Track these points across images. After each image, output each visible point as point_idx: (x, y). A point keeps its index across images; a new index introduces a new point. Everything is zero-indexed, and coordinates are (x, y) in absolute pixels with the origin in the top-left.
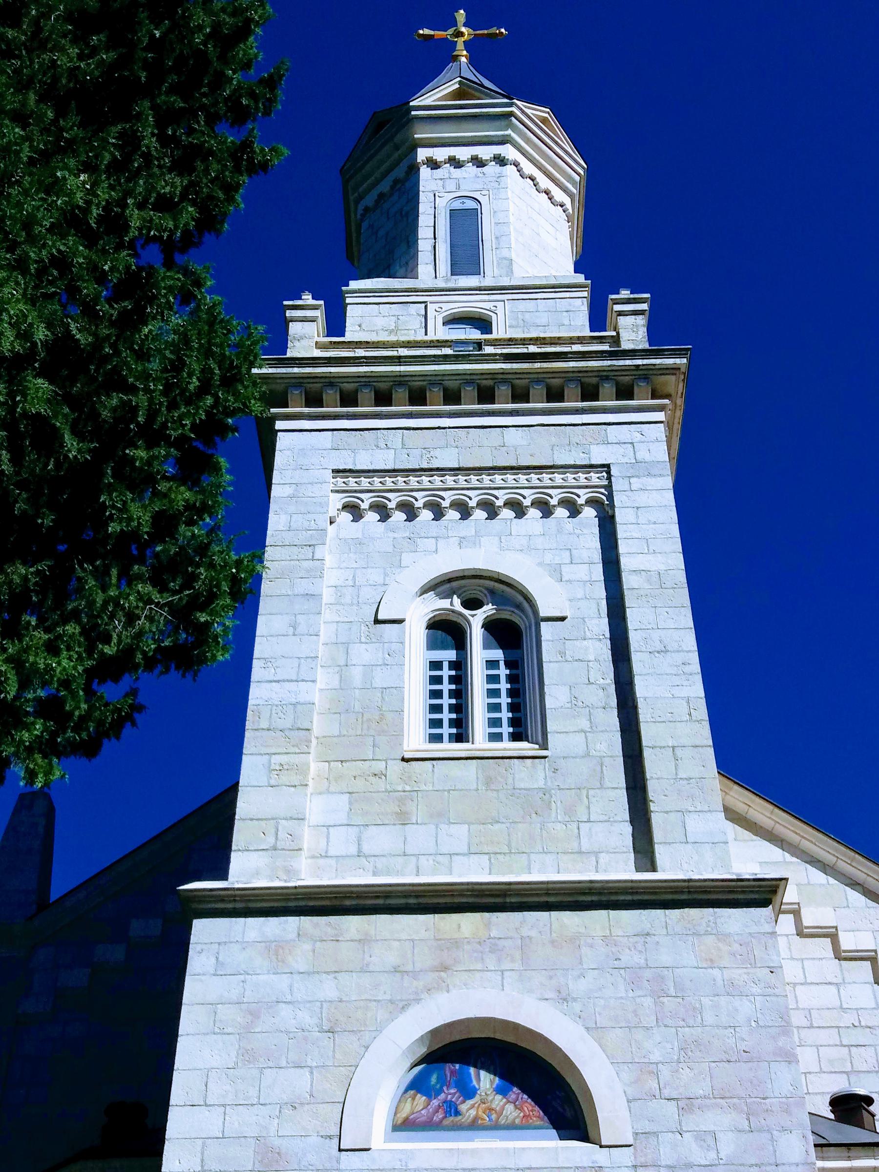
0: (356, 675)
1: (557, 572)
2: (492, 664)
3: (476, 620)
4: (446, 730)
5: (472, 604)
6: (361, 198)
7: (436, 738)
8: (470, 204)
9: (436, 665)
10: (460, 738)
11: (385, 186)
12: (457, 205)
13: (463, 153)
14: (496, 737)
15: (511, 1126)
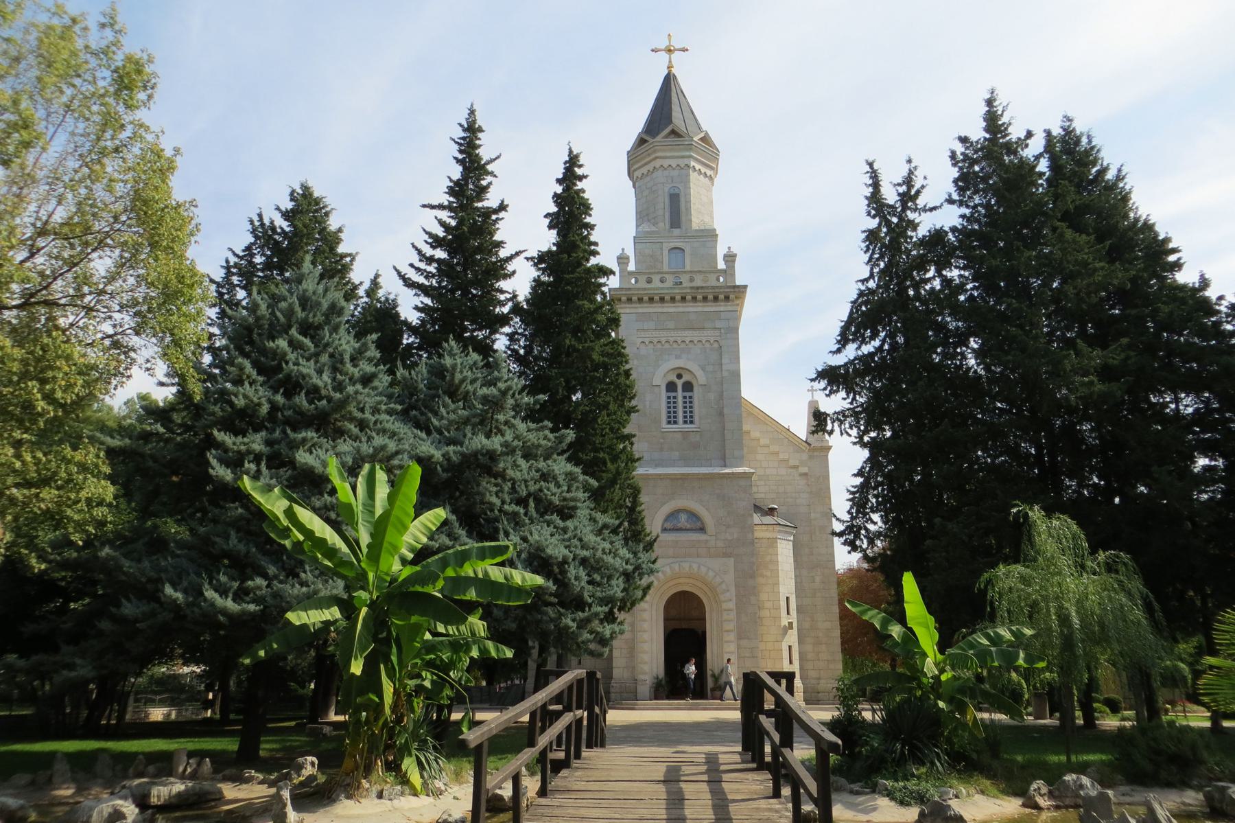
0: (648, 403)
1: (703, 369)
2: (685, 397)
3: (680, 383)
4: (672, 420)
5: (679, 376)
6: (635, 170)
7: (669, 422)
8: (677, 191)
9: (669, 398)
10: (675, 422)
11: (644, 170)
12: (672, 192)
13: (673, 163)
14: (685, 422)
15: (687, 530)
